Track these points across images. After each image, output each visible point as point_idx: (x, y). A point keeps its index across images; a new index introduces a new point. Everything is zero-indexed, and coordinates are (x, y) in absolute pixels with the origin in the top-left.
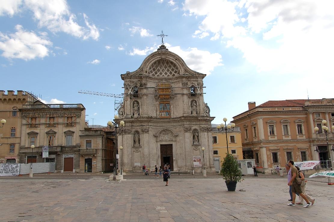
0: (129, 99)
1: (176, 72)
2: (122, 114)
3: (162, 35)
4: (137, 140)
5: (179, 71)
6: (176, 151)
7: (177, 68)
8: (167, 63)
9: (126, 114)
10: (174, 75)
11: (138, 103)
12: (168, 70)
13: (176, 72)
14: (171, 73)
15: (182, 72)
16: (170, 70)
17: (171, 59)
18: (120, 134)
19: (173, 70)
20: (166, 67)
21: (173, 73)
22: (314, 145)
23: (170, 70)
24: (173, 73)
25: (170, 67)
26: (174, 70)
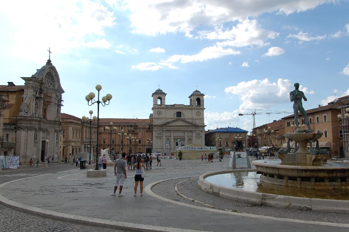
0: (35, 101)
1: (51, 84)
2: (27, 113)
3: (50, 52)
4: (36, 137)
5: (55, 85)
6: (48, 147)
7: (54, 82)
8: (49, 76)
9: (31, 112)
10: (49, 86)
11: (37, 105)
12: (47, 81)
13: (51, 84)
14: (48, 84)
15: (56, 87)
16: (48, 81)
17: (53, 73)
18: (23, 130)
19: (50, 82)
20: (47, 78)
21: (49, 84)
22: (84, 145)
23: (48, 81)
24: (49, 84)
25: (49, 79)
26: (51, 83)
